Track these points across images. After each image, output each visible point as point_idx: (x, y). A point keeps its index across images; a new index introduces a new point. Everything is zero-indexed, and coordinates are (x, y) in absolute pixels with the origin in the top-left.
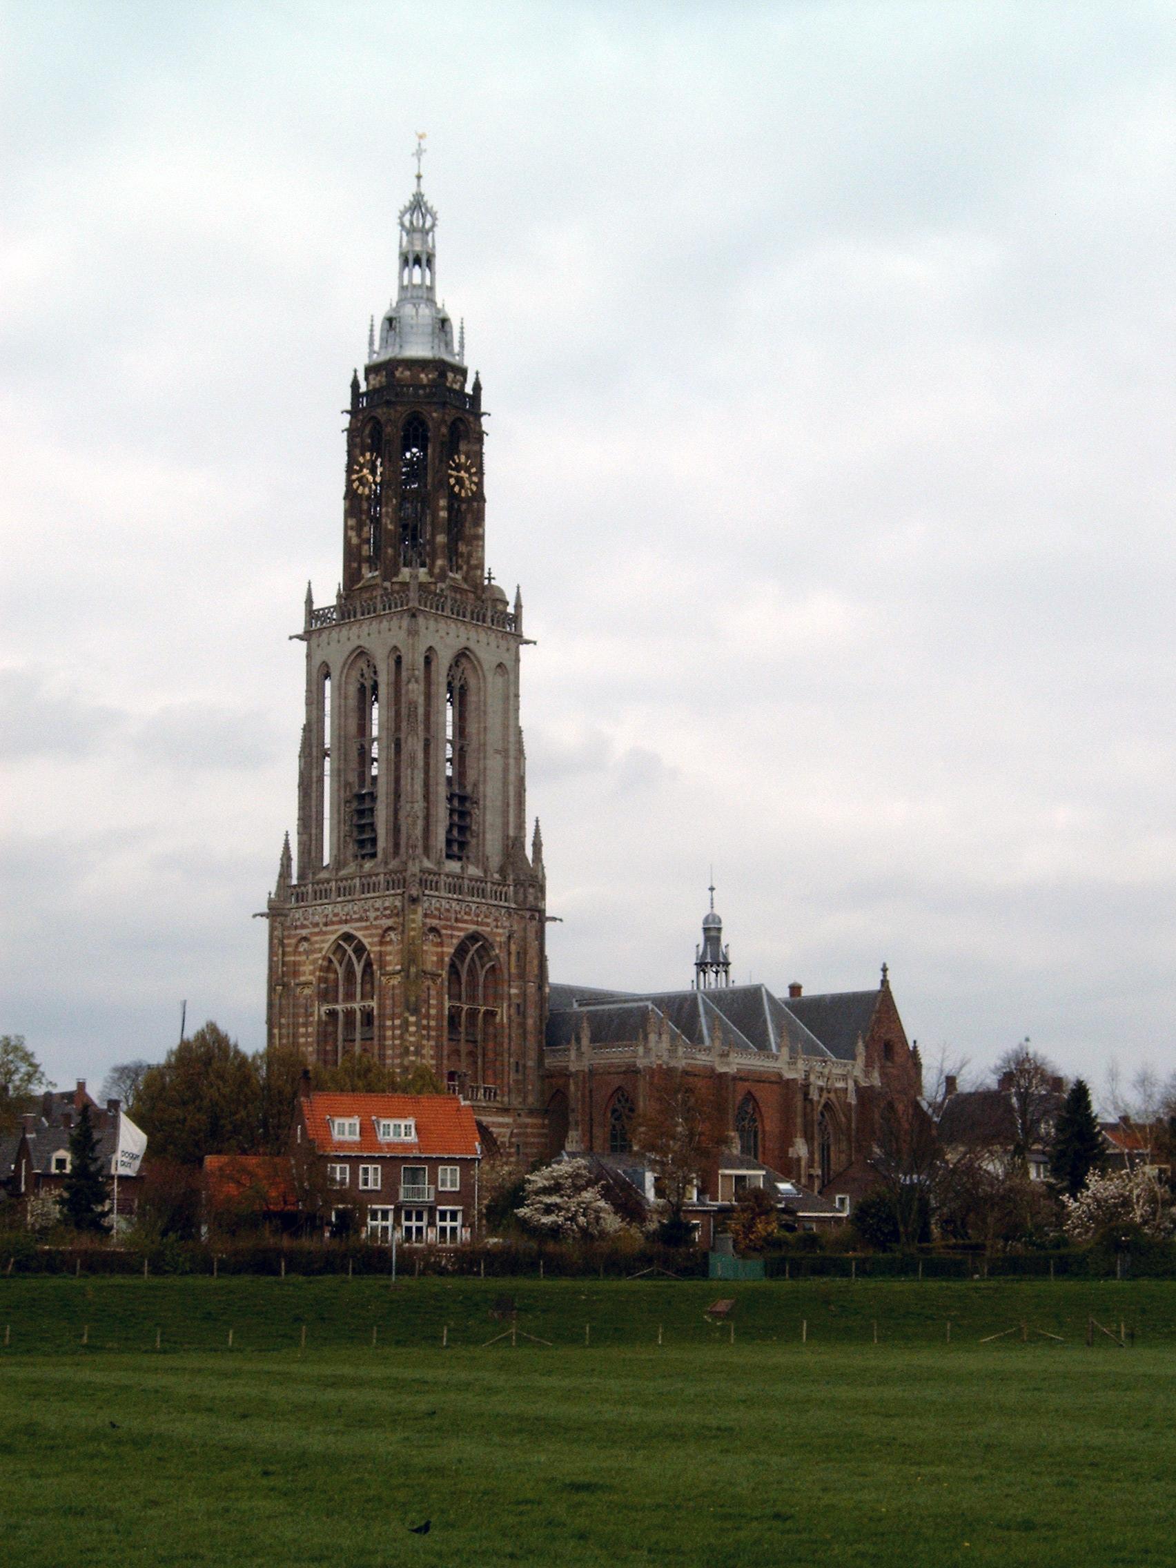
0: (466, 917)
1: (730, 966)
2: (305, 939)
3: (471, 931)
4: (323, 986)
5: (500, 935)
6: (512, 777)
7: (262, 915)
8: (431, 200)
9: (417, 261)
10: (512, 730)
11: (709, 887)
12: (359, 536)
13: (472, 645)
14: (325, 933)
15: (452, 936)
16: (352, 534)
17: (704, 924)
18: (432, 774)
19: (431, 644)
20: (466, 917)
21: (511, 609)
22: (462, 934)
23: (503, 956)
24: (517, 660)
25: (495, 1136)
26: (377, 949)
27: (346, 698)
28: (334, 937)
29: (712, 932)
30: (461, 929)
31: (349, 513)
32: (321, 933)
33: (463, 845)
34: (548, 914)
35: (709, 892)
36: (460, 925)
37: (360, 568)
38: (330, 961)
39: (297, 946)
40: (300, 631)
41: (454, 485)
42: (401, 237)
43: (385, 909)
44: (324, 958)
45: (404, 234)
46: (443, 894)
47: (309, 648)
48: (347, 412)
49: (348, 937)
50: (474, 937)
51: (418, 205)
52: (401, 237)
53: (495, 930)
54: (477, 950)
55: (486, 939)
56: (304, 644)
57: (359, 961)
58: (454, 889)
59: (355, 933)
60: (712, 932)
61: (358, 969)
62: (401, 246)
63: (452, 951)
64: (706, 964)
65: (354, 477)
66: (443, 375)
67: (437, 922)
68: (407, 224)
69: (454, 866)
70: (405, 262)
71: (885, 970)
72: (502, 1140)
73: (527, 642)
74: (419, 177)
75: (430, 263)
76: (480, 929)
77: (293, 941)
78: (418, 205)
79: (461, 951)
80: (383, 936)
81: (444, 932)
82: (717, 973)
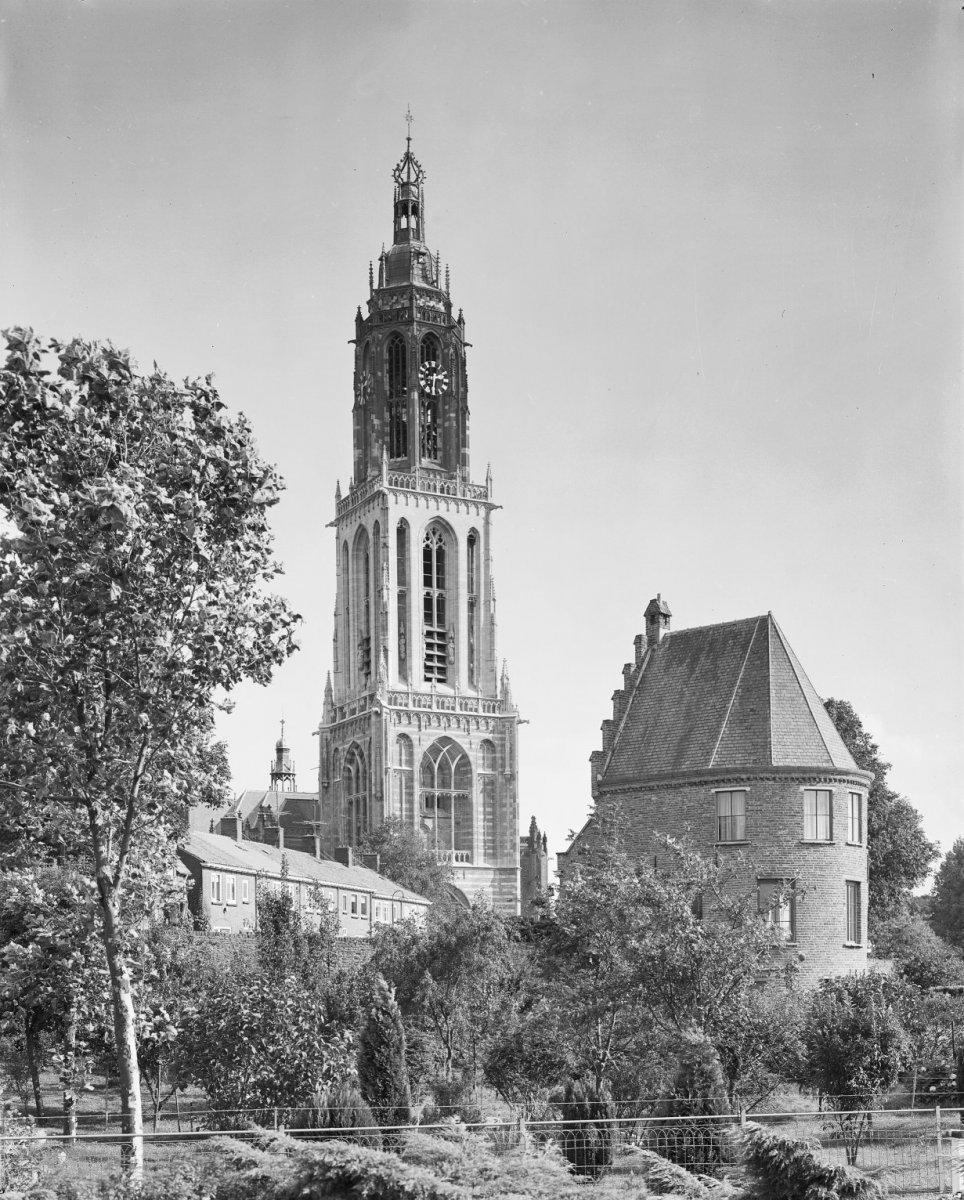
8: (417, 157)
47: (338, 529)
74: (409, 139)
75: (415, 211)
79: (434, 750)
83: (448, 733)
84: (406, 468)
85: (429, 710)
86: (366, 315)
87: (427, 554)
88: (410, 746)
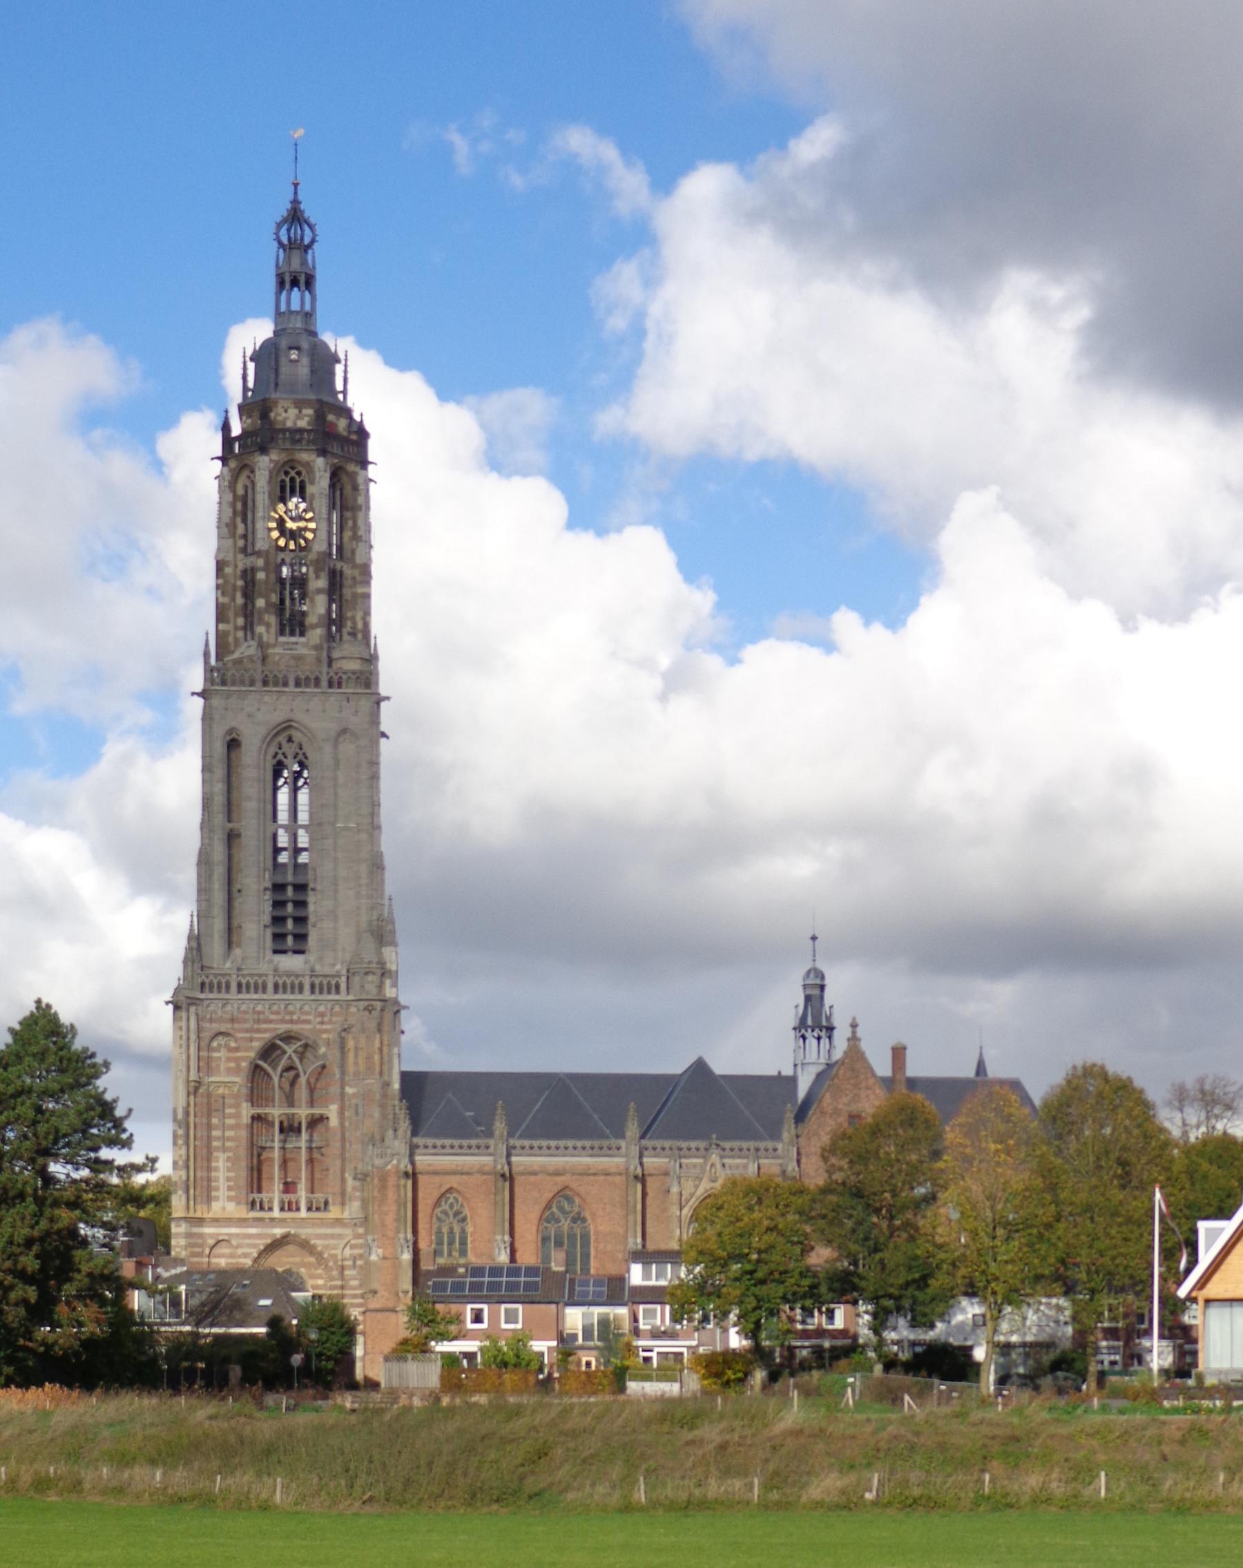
1: (835, 1032)
3: (281, 1031)
5: (326, 1031)
8: (309, 210)
9: (295, 283)
11: (810, 935)
13: (299, 716)
15: (251, 1040)
17: (804, 980)
19: (234, 724)
20: (273, 1017)
22: (267, 1036)
23: (333, 1057)
25: (319, 1249)
30: (266, 1031)
33: (301, 937)
35: (811, 942)
41: (277, 539)
42: (278, 256)
45: (281, 251)
50: (288, 1038)
51: (295, 216)
52: (278, 256)
53: (318, 1027)
62: (277, 266)
63: (252, 1054)
67: (229, 1026)
68: (285, 240)
70: (281, 284)
72: (333, 1252)
75: (309, 282)
76: (295, 1027)
78: (295, 216)
81: (240, 1035)
82: (819, 1038)
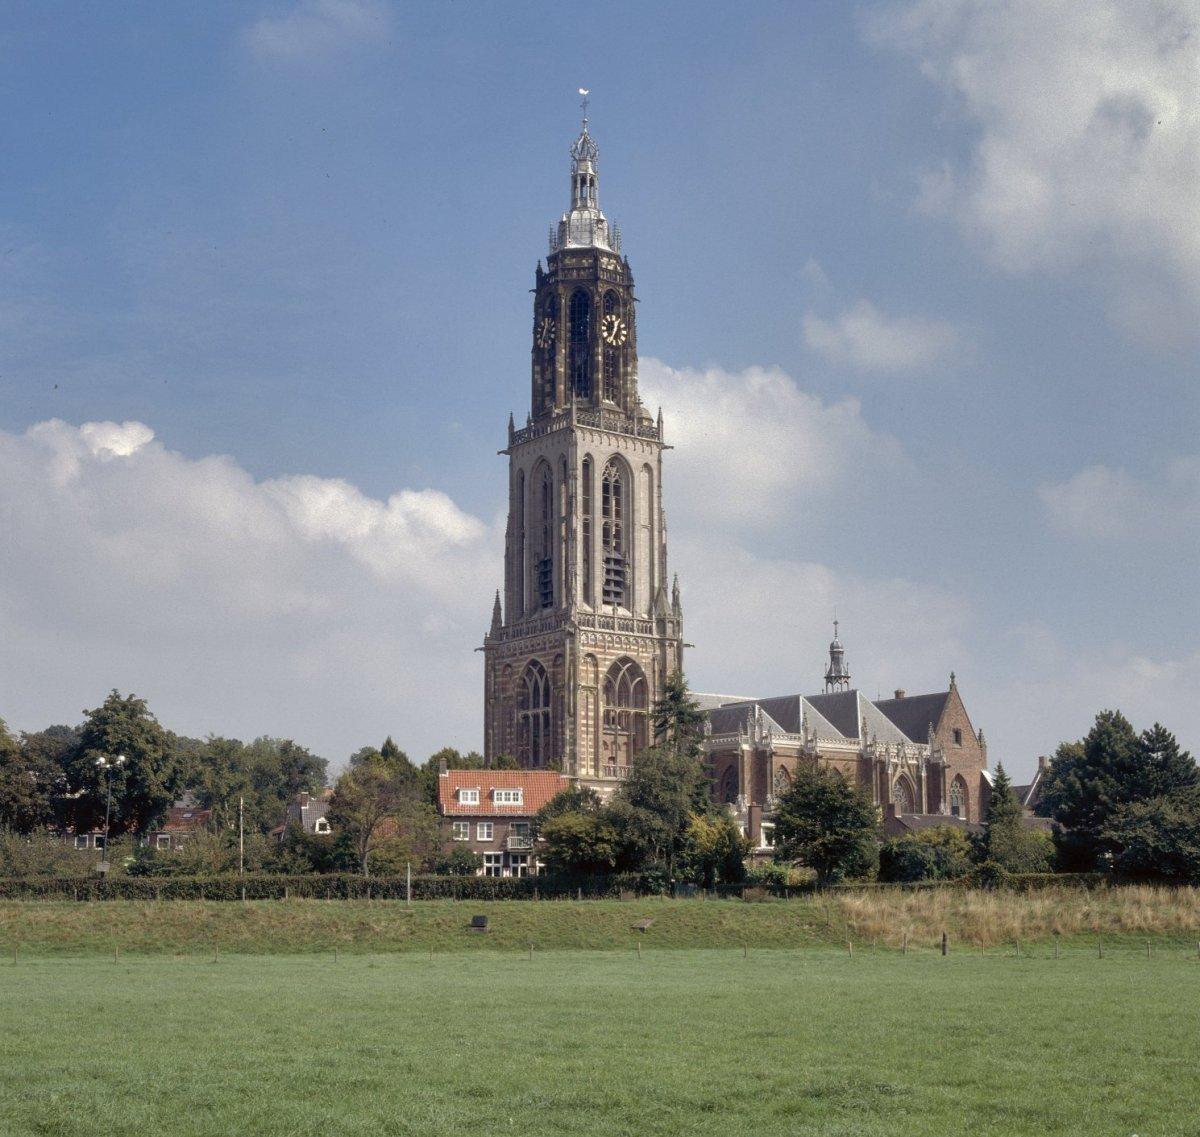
0: (616, 646)
2: (509, 665)
4: (521, 698)
6: (656, 544)
7: (481, 649)
10: (656, 511)
12: (543, 378)
13: (622, 451)
14: (521, 660)
15: (605, 659)
16: (537, 376)
18: (591, 543)
21: (655, 425)
24: (660, 461)
26: (551, 670)
27: (534, 493)
28: (525, 663)
29: (835, 655)
30: (612, 654)
31: (535, 363)
32: (518, 660)
34: (685, 642)
36: (612, 651)
37: (543, 401)
38: (524, 680)
39: (504, 671)
40: (506, 448)
43: (556, 641)
44: (521, 678)
46: (598, 629)
47: (511, 460)
48: (533, 291)
49: (534, 663)
50: (625, 660)
54: (628, 669)
55: (634, 662)
56: (508, 457)
57: (541, 678)
58: (606, 625)
59: (539, 660)
60: (835, 655)
61: (541, 685)
63: (606, 670)
64: (831, 677)
65: (539, 336)
66: (596, 259)
69: (608, 609)
71: (953, 677)
73: (666, 447)
77: (501, 667)
79: (614, 669)
80: (555, 661)
81: (599, 656)
83: (629, 654)
84: (594, 405)
85: (612, 631)
86: (546, 270)
87: (606, 488)
88: (596, 665)
